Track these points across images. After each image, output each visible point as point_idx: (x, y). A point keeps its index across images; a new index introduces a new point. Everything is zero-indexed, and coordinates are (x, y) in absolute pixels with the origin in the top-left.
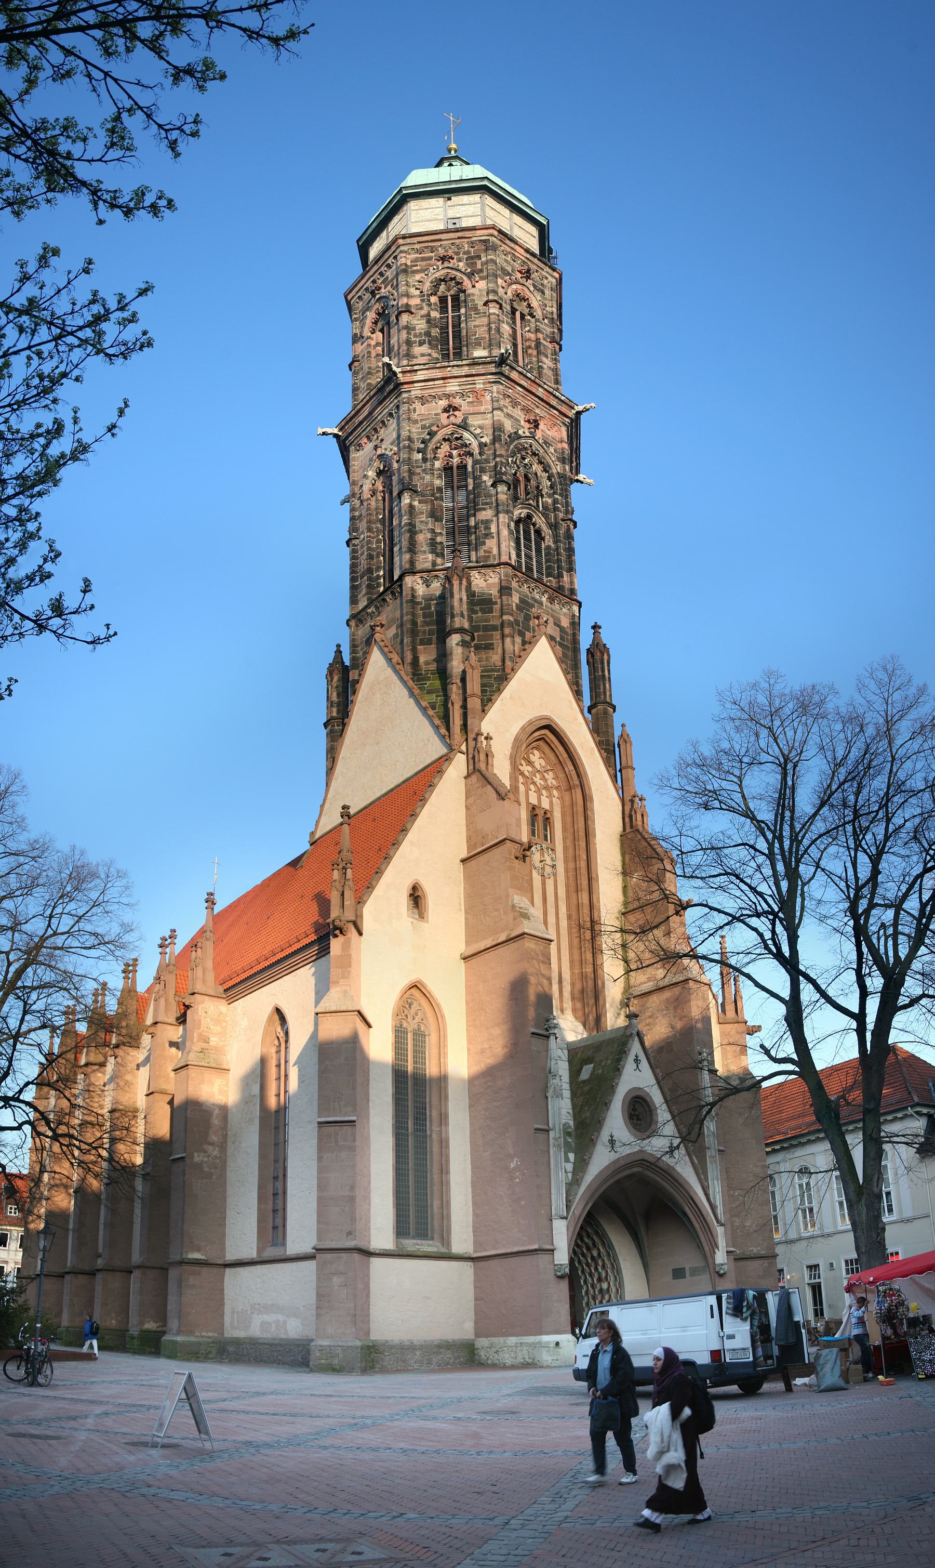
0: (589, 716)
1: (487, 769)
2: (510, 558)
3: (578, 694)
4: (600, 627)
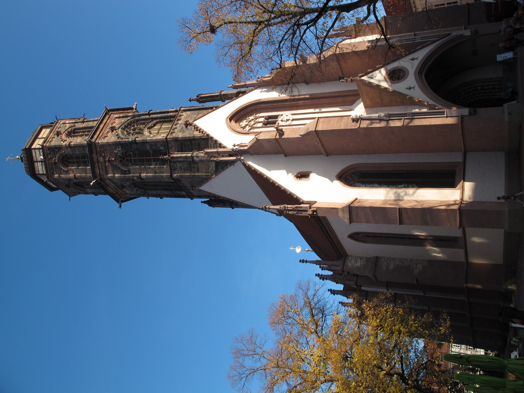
0: (226, 102)
1: (247, 146)
2: (164, 137)
3: (217, 108)
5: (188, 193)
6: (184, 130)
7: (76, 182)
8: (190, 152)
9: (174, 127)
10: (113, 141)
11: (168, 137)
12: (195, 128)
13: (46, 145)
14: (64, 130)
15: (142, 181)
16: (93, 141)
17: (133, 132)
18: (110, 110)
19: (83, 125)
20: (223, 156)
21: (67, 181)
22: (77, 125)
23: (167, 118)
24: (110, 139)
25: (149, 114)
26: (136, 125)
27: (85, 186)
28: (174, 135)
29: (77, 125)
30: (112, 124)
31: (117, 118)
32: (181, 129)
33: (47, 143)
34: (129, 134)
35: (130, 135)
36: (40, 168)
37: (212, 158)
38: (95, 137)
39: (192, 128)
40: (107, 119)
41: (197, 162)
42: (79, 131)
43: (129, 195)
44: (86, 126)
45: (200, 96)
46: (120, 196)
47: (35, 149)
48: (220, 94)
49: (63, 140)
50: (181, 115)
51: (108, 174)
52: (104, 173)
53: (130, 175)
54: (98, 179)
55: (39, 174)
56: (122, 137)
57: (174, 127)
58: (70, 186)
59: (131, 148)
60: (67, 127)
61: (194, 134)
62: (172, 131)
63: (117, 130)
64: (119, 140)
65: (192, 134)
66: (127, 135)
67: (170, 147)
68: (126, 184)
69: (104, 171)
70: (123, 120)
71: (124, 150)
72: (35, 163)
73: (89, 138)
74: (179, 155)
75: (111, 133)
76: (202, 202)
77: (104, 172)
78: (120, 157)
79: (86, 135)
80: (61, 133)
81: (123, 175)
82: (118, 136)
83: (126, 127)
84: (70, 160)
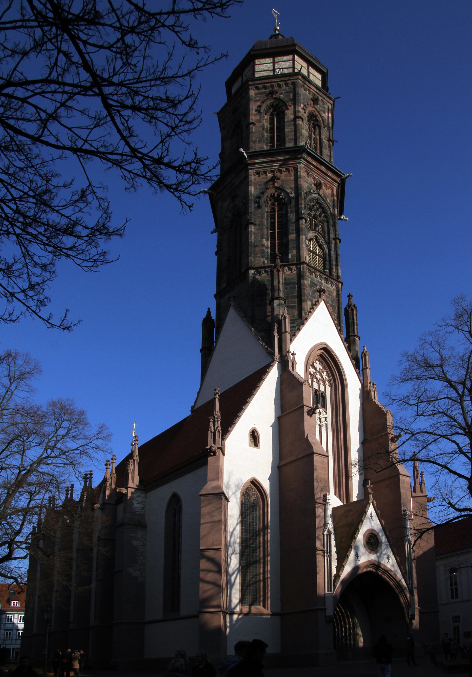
2: (306, 259)
14: (319, 110)
19: (325, 139)
24: (305, 181)
36: (264, 67)
38: (309, 159)
44: (324, 145)
47: (294, 60)
57: (318, 274)
60: (323, 115)
62: (313, 270)
82: (308, 193)
83: (320, 204)
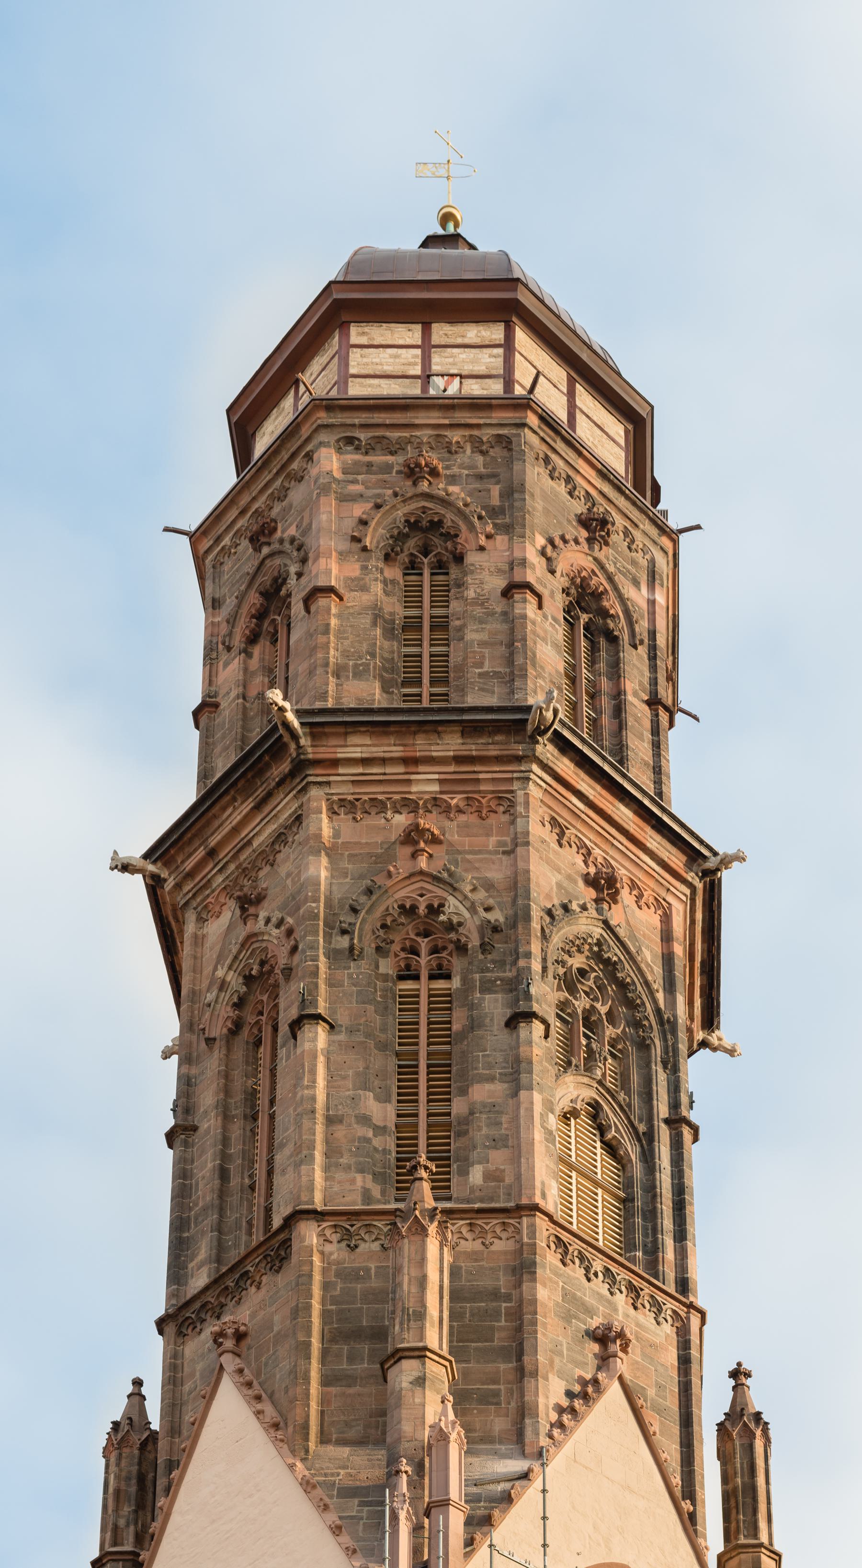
2: (544, 1196)
4: (748, 1375)
5: (197, 1305)
6: (578, 1319)
7: (289, 595)
8: (451, 1341)
9: (598, 1265)
10: (532, 875)
11: (541, 1222)
12: (584, 1383)
13: (526, 430)
14: (611, 569)
15: (284, 1029)
16: (539, 748)
17: (580, 1011)
18: (712, 883)
19: (635, 694)
20: (417, 1529)
21: (292, 531)
22: (635, 662)
23: (645, 1228)
24: (549, 862)
25: (676, 1121)
26: (619, 1031)
27: (256, 651)
28: (549, 1258)
29: (635, 662)
30: (633, 885)
31: (666, 919)
32: (583, 1304)
33: (543, 439)
34: (569, 983)
35: (559, 989)
36: (384, 360)
37: (409, 1469)
38: (565, 767)
39: (583, 1365)
40: (664, 855)
41: (391, 1374)
42: (602, 666)
43: (195, 936)
44: (630, 721)
45: (758, 1433)
46: (190, 875)
47: (508, 345)
48: (761, 1545)
49: (554, 546)
50: (657, 1308)
51: (335, 813)
52: (343, 789)
53: (322, 958)
54: (302, 742)
55: (347, 347)
56: (557, 940)
57: (598, 1265)
58: (265, 550)
59: (487, 987)
60: (630, 592)
61: (550, 1376)
62: (575, 1246)
63: (594, 914)
64: (536, 913)
65: (552, 1363)
66: (561, 971)
67: (479, 1222)
68: (268, 921)
69: (352, 789)
70: (655, 974)
71: (474, 941)
72: (419, 327)
73: (556, 726)
74: (433, 1275)
75: (577, 872)
76: (138, 1383)
77: (346, 791)
78: (434, 910)
79: (574, 707)
80: (597, 547)
81: (322, 915)
82: (559, 912)
83: (610, 967)
84: (426, 573)
